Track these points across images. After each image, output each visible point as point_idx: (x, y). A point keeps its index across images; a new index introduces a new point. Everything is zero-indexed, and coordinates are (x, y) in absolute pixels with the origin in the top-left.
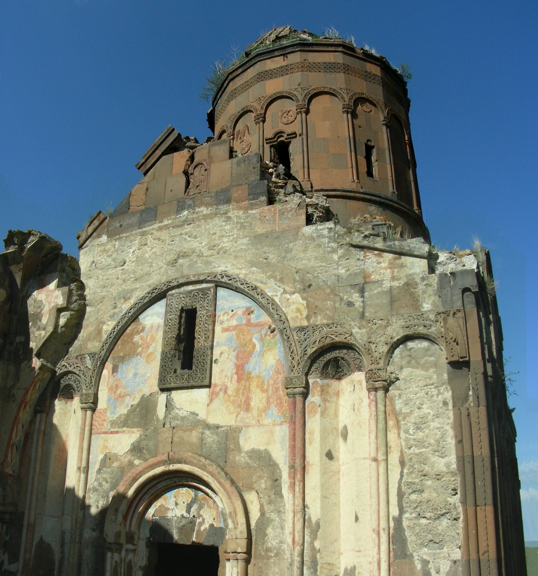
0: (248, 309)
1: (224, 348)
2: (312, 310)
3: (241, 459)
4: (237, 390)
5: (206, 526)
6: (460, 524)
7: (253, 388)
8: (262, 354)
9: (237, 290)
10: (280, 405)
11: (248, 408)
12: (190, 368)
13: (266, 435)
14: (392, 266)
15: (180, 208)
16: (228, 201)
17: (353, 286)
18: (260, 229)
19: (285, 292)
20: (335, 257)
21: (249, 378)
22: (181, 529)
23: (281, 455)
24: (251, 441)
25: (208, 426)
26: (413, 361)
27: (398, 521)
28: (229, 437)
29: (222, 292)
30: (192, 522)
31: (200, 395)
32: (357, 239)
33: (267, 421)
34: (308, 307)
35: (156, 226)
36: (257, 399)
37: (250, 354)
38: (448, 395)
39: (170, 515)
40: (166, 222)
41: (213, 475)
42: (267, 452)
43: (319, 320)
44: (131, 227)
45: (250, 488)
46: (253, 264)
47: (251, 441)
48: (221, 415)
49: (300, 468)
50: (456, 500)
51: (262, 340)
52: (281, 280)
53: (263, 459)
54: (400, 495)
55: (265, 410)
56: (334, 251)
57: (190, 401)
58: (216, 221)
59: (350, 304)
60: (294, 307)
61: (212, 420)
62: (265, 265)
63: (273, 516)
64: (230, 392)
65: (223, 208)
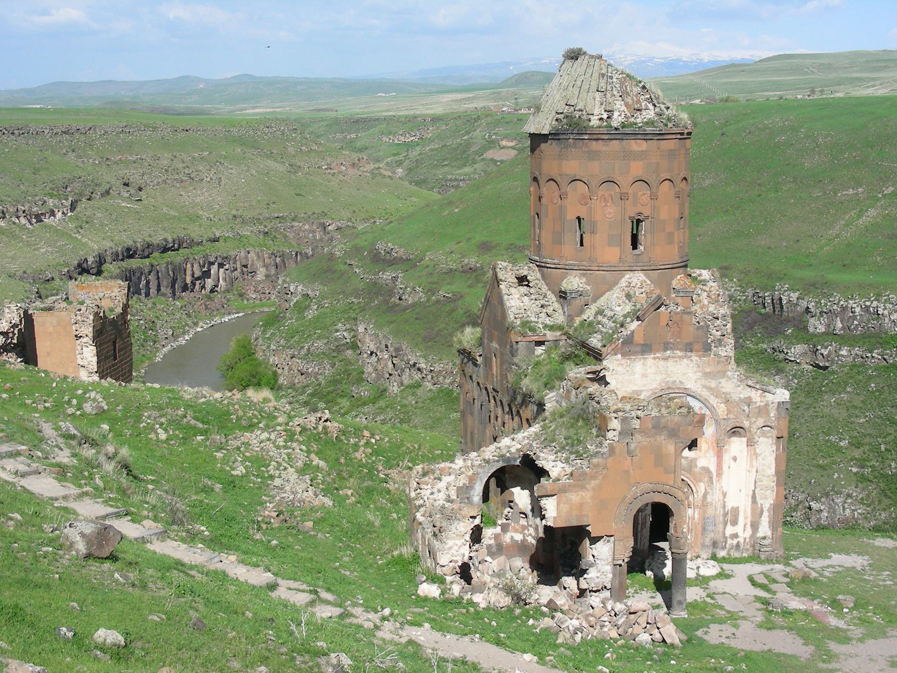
2: (729, 412)
6: (775, 493)
10: (713, 449)
14: (761, 396)
15: (665, 349)
16: (691, 351)
18: (708, 370)
20: (739, 389)
23: (713, 469)
24: (701, 463)
26: (764, 435)
27: (754, 491)
32: (750, 383)
33: (708, 455)
34: (728, 410)
35: (652, 356)
38: (774, 448)
40: (658, 355)
43: (731, 416)
44: (635, 353)
45: (701, 481)
46: (704, 387)
49: (719, 474)
50: (774, 484)
53: (706, 470)
54: (755, 482)
55: (707, 451)
56: (739, 386)
58: (685, 360)
59: (744, 411)
60: (721, 410)
62: (710, 389)
65: (689, 354)
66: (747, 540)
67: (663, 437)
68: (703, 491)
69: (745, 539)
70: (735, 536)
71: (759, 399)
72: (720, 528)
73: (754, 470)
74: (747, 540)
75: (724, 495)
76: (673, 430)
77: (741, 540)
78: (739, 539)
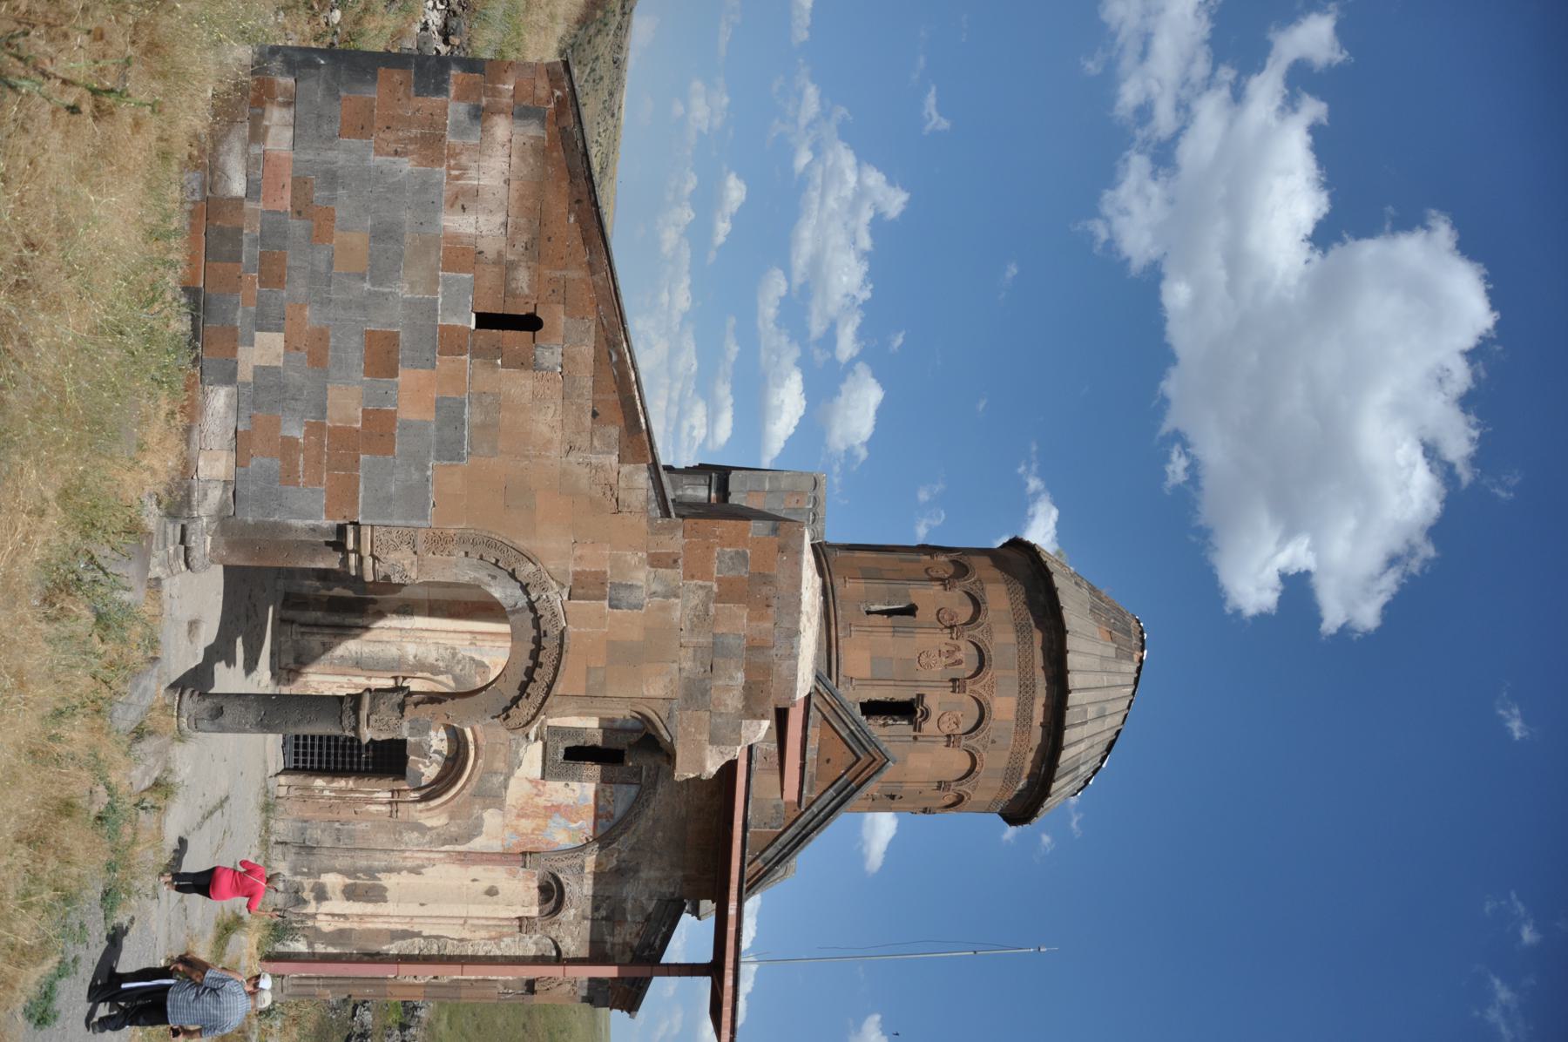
0: (612, 816)
1: (578, 792)
3: (476, 810)
4: (537, 806)
5: (423, 770)
7: (540, 822)
8: (567, 829)
9: (631, 808)
10: (519, 844)
11: (519, 816)
12: (566, 757)
13: (495, 831)
17: (613, 911)
19: (620, 852)
21: (547, 817)
22: (419, 745)
23: (477, 844)
24: (491, 819)
25: (507, 779)
27: (419, 935)
28: (494, 798)
29: (633, 790)
30: (426, 756)
31: (537, 772)
33: (507, 833)
36: (526, 825)
37: (570, 819)
39: (432, 733)
41: (463, 787)
42: (480, 833)
45: (451, 818)
47: (491, 819)
48: (517, 790)
49: (466, 859)
51: (580, 829)
52: (632, 849)
54: (438, 937)
55: (516, 831)
57: (532, 755)
61: (512, 782)
63: (427, 838)
64: (537, 800)
66: (310, 923)
67: (687, 665)
68: (429, 823)
69: (314, 916)
70: (321, 895)
71: (618, 940)
72: (341, 862)
73: (466, 934)
74: (310, 923)
75: (416, 871)
76: (705, 692)
77: (311, 908)
78: (313, 903)
